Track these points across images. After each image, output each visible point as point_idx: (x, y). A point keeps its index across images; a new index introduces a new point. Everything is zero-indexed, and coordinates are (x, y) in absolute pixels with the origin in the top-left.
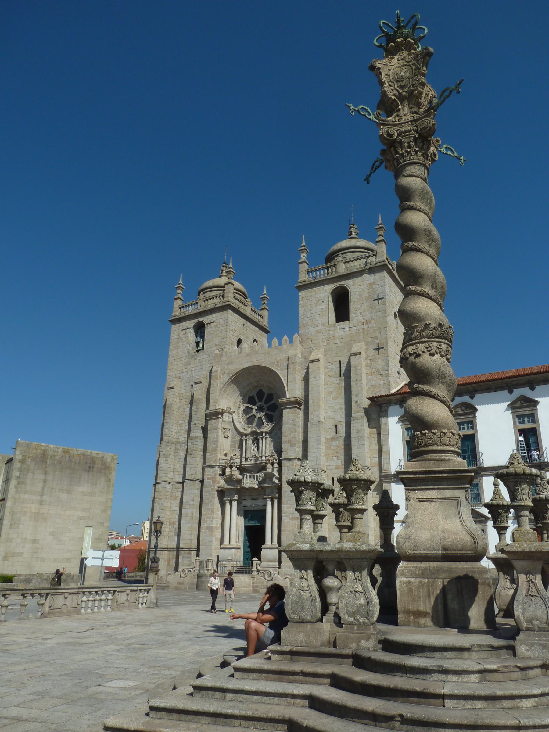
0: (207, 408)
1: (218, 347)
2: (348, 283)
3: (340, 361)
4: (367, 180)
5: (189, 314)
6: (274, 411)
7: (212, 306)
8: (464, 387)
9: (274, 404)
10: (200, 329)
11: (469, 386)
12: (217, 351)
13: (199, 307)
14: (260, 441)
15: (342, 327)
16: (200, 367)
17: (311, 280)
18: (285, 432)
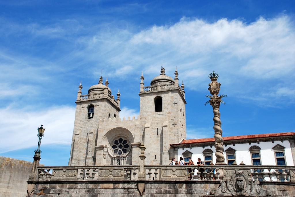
0: (96, 145)
1: (100, 117)
2: (162, 96)
3: (158, 128)
4: (205, 104)
5: (86, 100)
6: (127, 148)
7: (98, 98)
8: (208, 143)
9: (127, 144)
10: (91, 108)
11: (210, 143)
12: (101, 119)
13: (91, 98)
14: (121, 161)
15: (159, 114)
16: (91, 126)
17: (146, 92)
18: (133, 157)
